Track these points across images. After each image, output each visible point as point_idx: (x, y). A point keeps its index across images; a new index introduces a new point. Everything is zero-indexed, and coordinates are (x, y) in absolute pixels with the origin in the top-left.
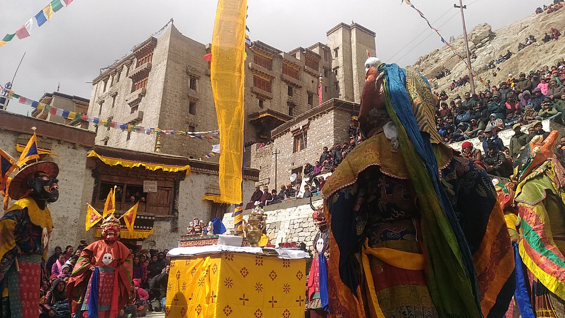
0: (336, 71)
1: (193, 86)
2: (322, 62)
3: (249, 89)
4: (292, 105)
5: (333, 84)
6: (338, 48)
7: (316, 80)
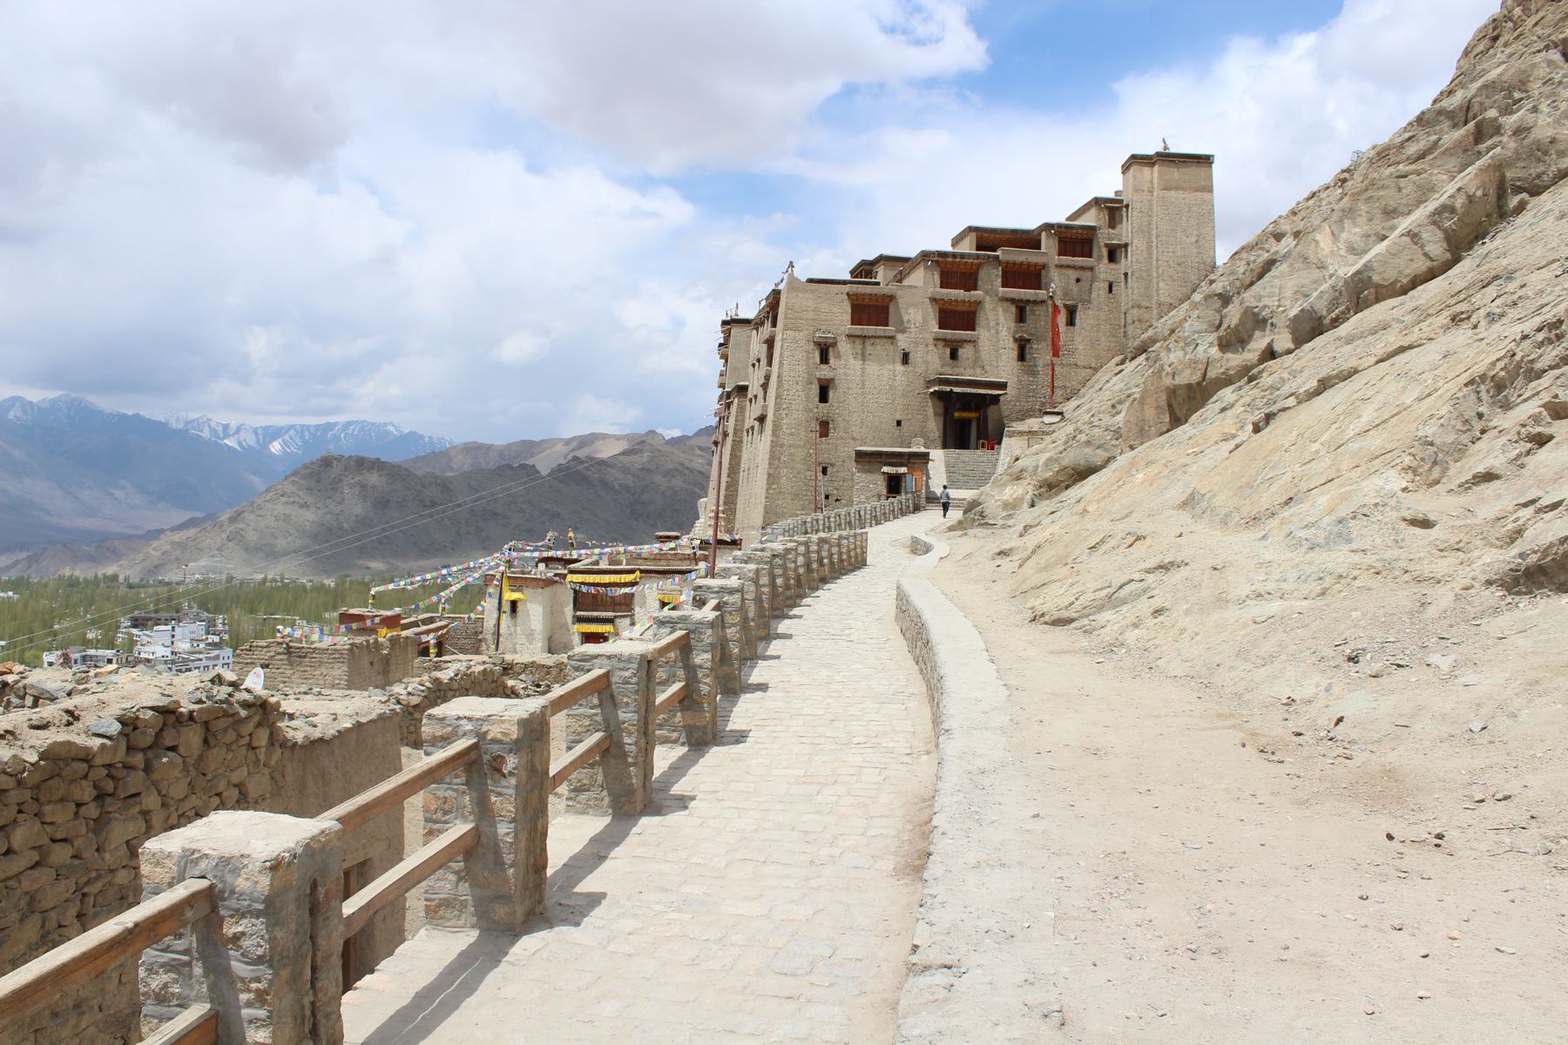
1: (824, 359)
2: (1105, 237)
7: (1086, 275)
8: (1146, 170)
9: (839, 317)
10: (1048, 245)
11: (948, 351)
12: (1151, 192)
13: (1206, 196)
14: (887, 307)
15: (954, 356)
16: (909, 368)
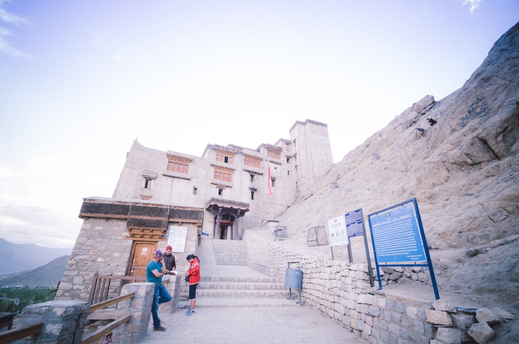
3: (209, 182)
4: (253, 191)
6: (295, 140)
7: (278, 166)
8: (302, 127)
9: (161, 166)
10: (264, 151)
11: (218, 190)
12: (305, 134)
16: (197, 196)
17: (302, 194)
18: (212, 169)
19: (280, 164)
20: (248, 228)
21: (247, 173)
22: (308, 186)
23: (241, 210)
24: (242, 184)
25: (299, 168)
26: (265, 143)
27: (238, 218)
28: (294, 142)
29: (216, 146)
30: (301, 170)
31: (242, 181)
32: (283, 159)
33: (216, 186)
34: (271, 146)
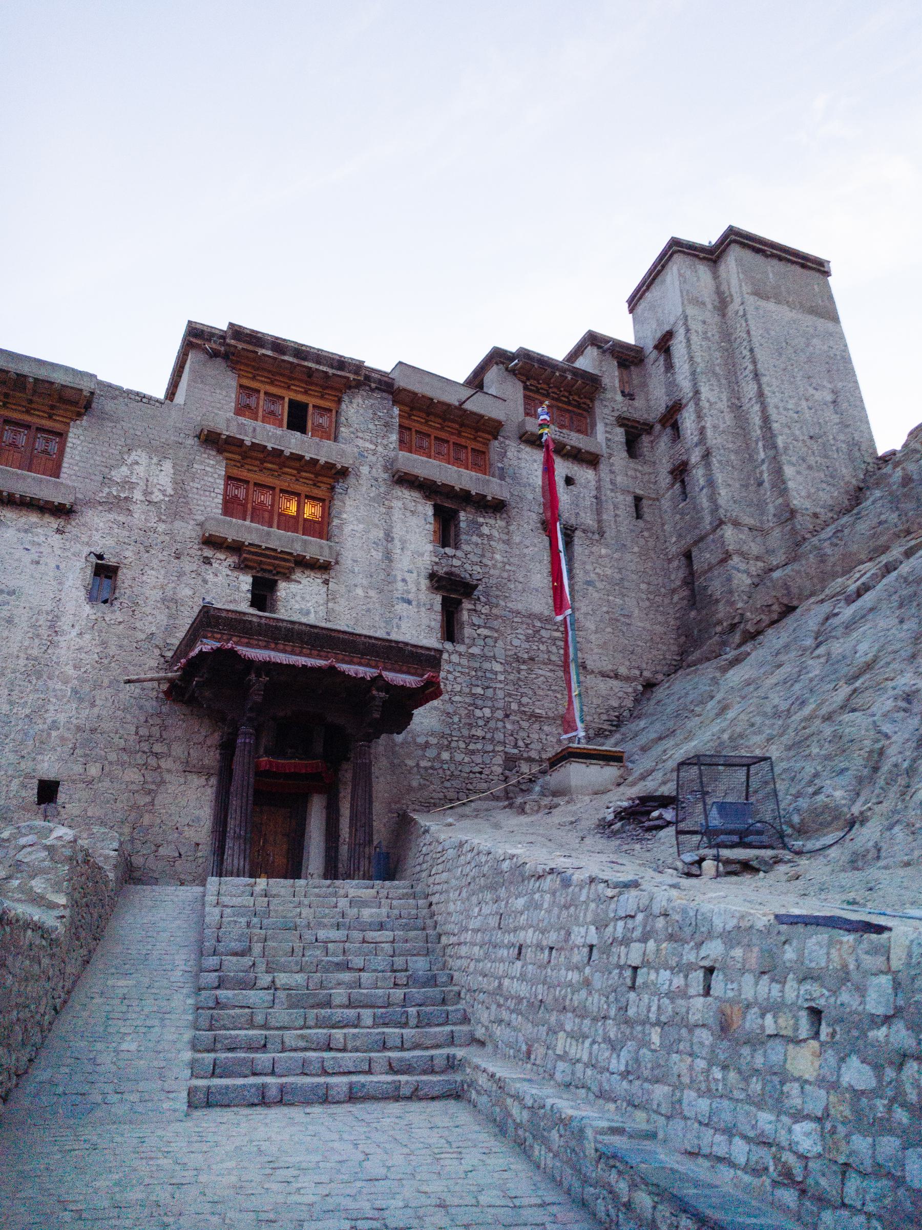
0: (676, 427)
2: (611, 404)
3: (187, 531)
5: (669, 479)
6: (668, 336)
7: (584, 475)
11: (246, 582)
12: (722, 303)
13: (830, 325)
14: (62, 436)
15: (263, 595)
16: (115, 615)
17: (722, 611)
18: (212, 471)
19: (592, 460)
20: (429, 806)
21: (416, 495)
22: (756, 567)
23: (388, 687)
24: (388, 556)
25: (698, 475)
26: (512, 348)
27: (371, 737)
28: (664, 344)
29: (237, 332)
30: (711, 483)
31: (389, 538)
32: (604, 435)
33: (232, 560)
34: (544, 363)
